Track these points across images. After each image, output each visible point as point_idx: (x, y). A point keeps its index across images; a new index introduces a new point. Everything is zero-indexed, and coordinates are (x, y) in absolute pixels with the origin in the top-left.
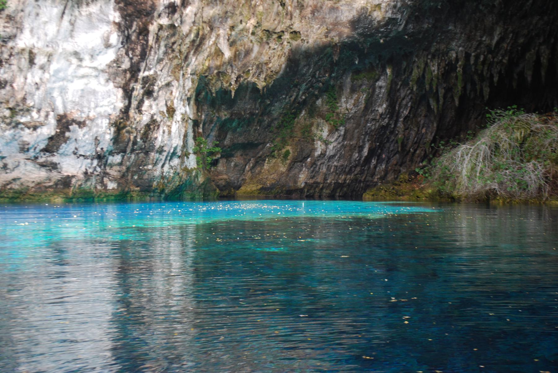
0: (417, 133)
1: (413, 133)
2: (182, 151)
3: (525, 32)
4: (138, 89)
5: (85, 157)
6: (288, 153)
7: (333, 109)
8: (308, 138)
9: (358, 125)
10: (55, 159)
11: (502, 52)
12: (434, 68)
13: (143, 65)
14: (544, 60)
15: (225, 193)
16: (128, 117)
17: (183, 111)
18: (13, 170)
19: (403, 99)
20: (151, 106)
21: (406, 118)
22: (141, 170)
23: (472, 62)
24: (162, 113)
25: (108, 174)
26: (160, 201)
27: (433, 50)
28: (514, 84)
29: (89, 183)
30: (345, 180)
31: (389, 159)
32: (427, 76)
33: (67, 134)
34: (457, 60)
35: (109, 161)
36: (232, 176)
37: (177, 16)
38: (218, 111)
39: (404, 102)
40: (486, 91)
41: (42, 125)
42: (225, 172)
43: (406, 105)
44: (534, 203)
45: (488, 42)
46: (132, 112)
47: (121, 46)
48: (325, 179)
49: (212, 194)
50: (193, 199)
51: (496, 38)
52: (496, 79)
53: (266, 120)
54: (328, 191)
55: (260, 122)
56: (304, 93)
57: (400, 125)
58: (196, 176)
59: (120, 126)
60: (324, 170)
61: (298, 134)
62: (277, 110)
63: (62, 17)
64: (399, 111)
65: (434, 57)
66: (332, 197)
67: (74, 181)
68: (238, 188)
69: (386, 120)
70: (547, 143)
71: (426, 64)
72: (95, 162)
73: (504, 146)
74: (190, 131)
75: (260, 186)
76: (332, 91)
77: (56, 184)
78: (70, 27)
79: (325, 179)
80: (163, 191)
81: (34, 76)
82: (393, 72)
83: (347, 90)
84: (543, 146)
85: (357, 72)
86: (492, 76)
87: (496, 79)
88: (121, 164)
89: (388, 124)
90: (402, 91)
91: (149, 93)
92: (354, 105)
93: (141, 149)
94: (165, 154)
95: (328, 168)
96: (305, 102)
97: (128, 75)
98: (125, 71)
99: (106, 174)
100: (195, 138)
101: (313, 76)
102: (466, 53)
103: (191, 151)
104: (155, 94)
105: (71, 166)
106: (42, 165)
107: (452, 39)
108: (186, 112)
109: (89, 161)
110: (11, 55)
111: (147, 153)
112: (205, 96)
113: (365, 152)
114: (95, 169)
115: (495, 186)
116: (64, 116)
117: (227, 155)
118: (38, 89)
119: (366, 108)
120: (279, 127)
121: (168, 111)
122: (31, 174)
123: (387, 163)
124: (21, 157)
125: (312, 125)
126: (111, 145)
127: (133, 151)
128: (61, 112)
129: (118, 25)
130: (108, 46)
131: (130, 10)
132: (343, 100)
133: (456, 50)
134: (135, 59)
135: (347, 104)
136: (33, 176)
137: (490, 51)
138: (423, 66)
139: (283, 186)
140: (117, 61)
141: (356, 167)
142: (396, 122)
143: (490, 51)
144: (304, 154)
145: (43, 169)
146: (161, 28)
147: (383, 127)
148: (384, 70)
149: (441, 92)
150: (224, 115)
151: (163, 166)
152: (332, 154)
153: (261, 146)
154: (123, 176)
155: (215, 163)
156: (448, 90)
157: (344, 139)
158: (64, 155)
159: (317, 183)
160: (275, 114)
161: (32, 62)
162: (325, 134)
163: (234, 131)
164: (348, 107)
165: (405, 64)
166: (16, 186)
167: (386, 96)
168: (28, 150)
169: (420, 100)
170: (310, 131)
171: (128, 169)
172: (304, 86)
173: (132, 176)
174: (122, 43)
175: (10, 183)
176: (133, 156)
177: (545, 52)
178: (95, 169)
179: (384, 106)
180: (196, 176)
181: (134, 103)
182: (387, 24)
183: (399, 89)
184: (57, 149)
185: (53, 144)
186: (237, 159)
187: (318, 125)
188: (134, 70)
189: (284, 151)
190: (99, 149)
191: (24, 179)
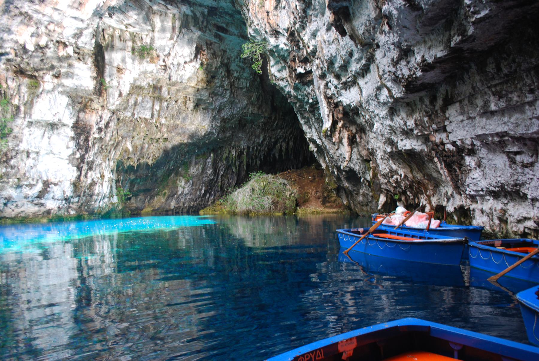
0: (228, 182)
1: (226, 182)
3: (275, 136)
4: (85, 167)
5: (58, 200)
6: (165, 193)
7: (186, 173)
8: (175, 186)
9: (199, 179)
10: (42, 201)
11: (264, 145)
12: (234, 153)
13: (86, 156)
14: (284, 149)
15: (135, 213)
16: (80, 181)
18: (21, 207)
20: (92, 175)
21: (222, 175)
23: (251, 150)
24: (98, 178)
25: (71, 207)
26: (99, 219)
27: (232, 145)
28: (271, 160)
29: (60, 212)
31: (215, 194)
34: (244, 149)
36: (139, 205)
37: (103, 133)
38: (130, 175)
40: (258, 163)
42: (134, 203)
44: (267, 215)
45: (258, 141)
46: (82, 178)
48: (184, 204)
49: (127, 214)
50: (116, 217)
51: (261, 140)
52: (262, 157)
54: (186, 210)
56: (173, 166)
57: (220, 179)
58: (118, 206)
59: (76, 185)
60: (183, 200)
61: (170, 184)
62: (160, 173)
63: (44, 135)
65: (233, 148)
66: (188, 213)
67: (52, 211)
68: (142, 210)
70: (274, 188)
71: (230, 151)
72: (64, 202)
73: (256, 189)
75: (152, 209)
76: (187, 165)
77: (43, 213)
79: (184, 204)
80: (100, 214)
81: (30, 162)
83: (193, 164)
84: (273, 189)
85: (198, 155)
86: (261, 156)
87: (262, 157)
88: (78, 202)
89: (213, 179)
91: (90, 168)
94: (100, 196)
95: (185, 199)
96: (173, 169)
97: (79, 161)
98: (78, 159)
99: (70, 207)
100: (116, 188)
101: (177, 158)
103: (115, 194)
104: (94, 169)
105: (51, 204)
106: (36, 204)
107: (241, 140)
110: (17, 154)
111: (91, 196)
112: (121, 169)
113: (203, 191)
114: (64, 205)
115: (251, 208)
116: (47, 181)
117: (136, 195)
118: (32, 168)
119: (202, 172)
120: (162, 181)
121: (101, 177)
122: (30, 209)
123: (214, 196)
124: (25, 201)
125: (177, 180)
127: (84, 196)
128: (45, 179)
129: (73, 138)
131: (79, 131)
132: (191, 168)
133: (243, 145)
134: (82, 153)
135: (193, 170)
137: (259, 145)
138: (228, 152)
139: (164, 208)
140: (74, 154)
141: (199, 198)
143: (259, 145)
145: (37, 206)
146: (95, 138)
148: (210, 155)
149: (237, 164)
150: (132, 177)
151: (100, 202)
154: (80, 207)
155: (129, 199)
156: (241, 163)
157: (193, 185)
158: (47, 199)
159: (180, 207)
160: (159, 175)
161: (28, 156)
162: (183, 183)
163: (139, 184)
165: (220, 151)
166: (23, 215)
167: (211, 166)
168: (28, 197)
169: (228, 168)
170: (176, 183)
171: (82, 204)
172: (172, 162)
175: (20, 213)
176: (84, 198)
177: (284, 145)
180: (118, 206)
181: (83, 173)
182: (209, 134)
184: (44, 196)
185: (41, 195)
186: (141, 197)
187: (180, 180)
188: (82, 158)
189: (164, 192)
190: (65, 196)
191: (27, 211)
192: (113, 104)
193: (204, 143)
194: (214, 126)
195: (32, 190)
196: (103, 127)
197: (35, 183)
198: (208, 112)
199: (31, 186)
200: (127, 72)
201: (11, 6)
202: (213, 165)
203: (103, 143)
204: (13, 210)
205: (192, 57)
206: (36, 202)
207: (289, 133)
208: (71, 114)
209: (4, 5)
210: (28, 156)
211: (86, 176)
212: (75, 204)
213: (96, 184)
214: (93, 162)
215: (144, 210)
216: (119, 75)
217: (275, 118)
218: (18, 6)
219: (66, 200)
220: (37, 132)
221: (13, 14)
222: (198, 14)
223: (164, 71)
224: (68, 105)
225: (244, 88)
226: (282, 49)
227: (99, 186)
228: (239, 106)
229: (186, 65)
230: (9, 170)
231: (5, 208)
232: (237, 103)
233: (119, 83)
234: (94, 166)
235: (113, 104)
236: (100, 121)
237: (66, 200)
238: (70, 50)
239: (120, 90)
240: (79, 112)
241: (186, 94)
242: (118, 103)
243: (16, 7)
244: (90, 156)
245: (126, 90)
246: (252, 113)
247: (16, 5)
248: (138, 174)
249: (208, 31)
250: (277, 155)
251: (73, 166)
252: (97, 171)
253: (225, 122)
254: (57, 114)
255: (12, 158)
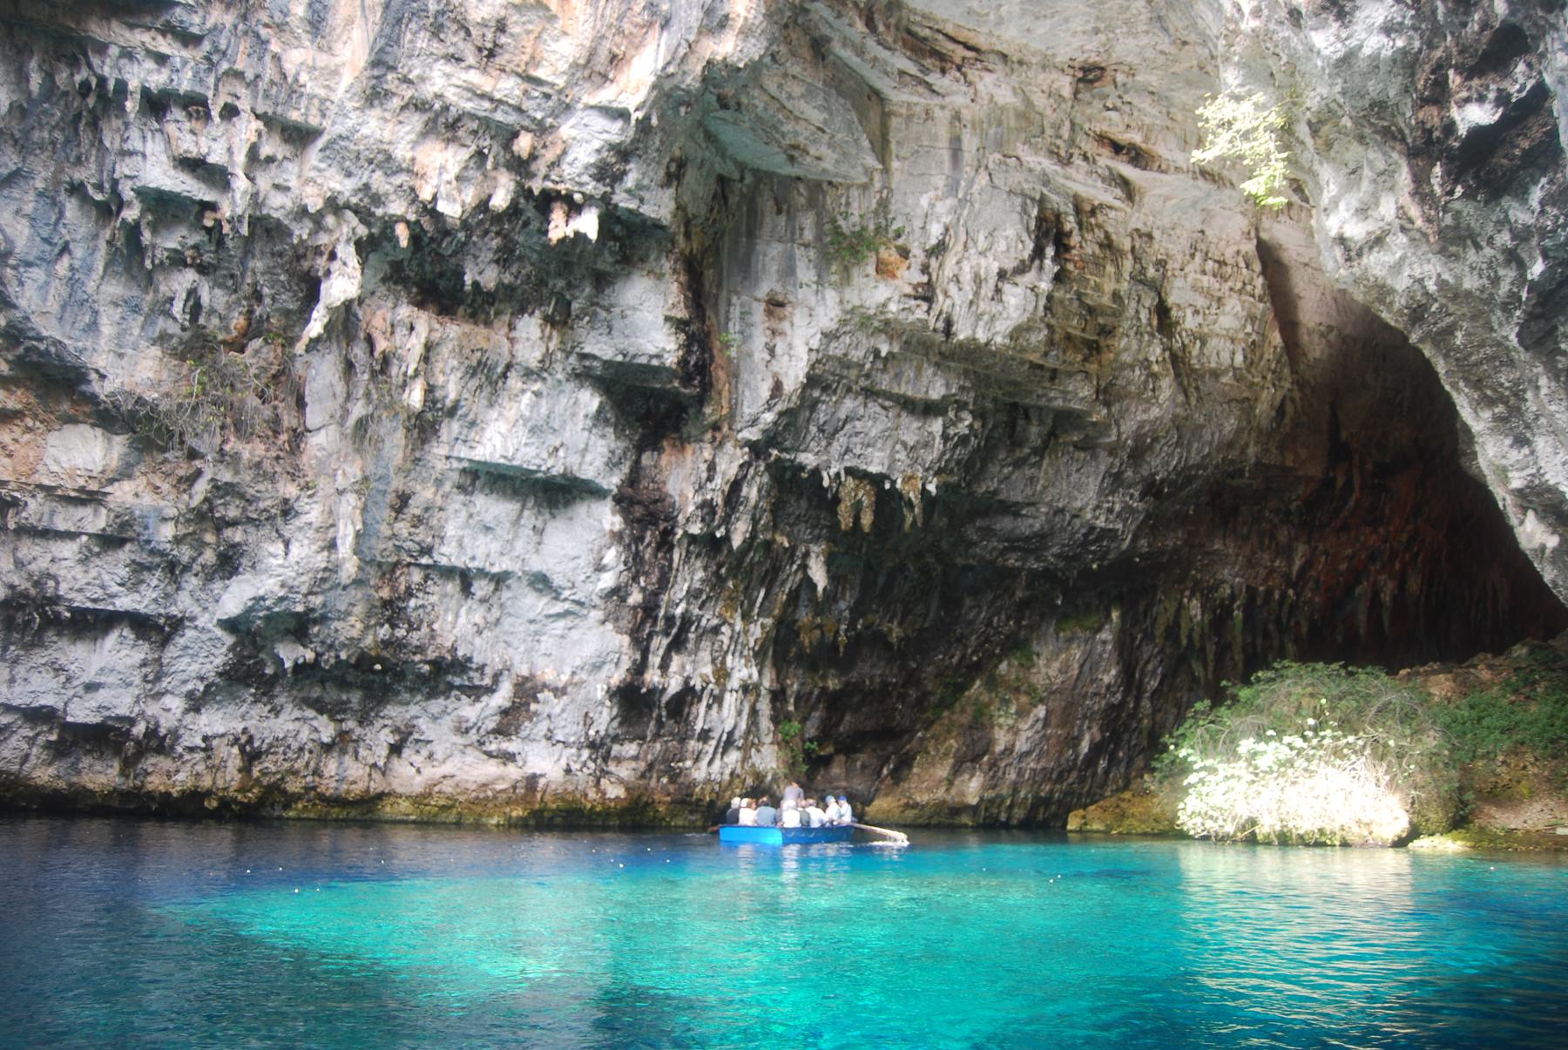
2: (746, 739)
10: (511, 746)
14: (1386, 598)
17: (744, 673)
19: (1148, 662)
22: (673, 769)
23: (1259, 602)
30: (1051, 792)
32: (1183, 624)
33: (533, 707)
34: (1233, 597)
35: (613, 753)
38: (824, 678)
39: (1150, 667)
41: (490, 690)
43: (1154, 672)
46: (652, 677)
47: (622, 567)
51: (1298, 564)
52: (1304, 629)
53: (913, 693)
55: (902, 697)
56: (974, 653)
57: (1146, 704)
60: (1012, 776)
64: (1141, 680)
67: (542, 782)
69: (1119, 696)
71: (1181, 605)
72: (586, 753)
74: (764, 707)
78: (536, 538)
82: (1123, 617)
86: (1298, 623)
88: (636, 758)
89: (1123, 703)
90: (1145, 648)
91: (677, 645)
92: (1060, 671)
93: (671, 734)
94: (713, 743)
95: (1020, 773)
98: (634, 608)
99: (605, 773)
100: (775, 719)
101: (989, 624)
102: (1248, 587)
104: (690, 646)
106: (490, 755)
108: (750, 677)
109: (574, 750)
110: (426, 578)
111: (682, 741)
113: (1085, 747)
118: (479, 632)
126: (615, 724)
128: (525, 672)
129: (617, 537)
130: (600, 568)
133: (1231, 578)
136: (476, 772)
140: (618, 593)
141: (1070, 771)
142: (1138, 700)
144: (978, 750)
145: (493, 761)
146: (693, 539)
147: (1112, 707)
148: (1108, 616)
149: (1211, 649)
151: (710, 763)
152: (1025, 748)
153: (906, 737)
154: (643, 776)
161: (466, 589)
164: (1051, 673)
166: (447, 787)
168: (467, 731)
171: (651, 766)
173: (659, 778)
174: (625, 563)
178: (585, 764)
179: (1113, 672)
181: (655, 660)
182: (1098, 540)
183: (1139, 646)
188: (649, 609)
190: (592, 732)
191: (460, 776)
192: (754, 422)
193: (1086, 573)
194: (1117, 507)
195: (479, 706)
196: (719, 500)
197: (487, 681)
198: (1094, 457)
199: (476, 693)
200: (799, 317)
201: (390, 77)
202: (1121, 655)
203: (721, 558)
204: (418, 771)
205: (1026, 255)
206: (493, 747)
207: (1404, 537)
208: (613, 452)
209: (368, 73)
210: (466, 589)
211: (664, 667)
212: (625, 764)
213: (700, 700)
214: (687, 621)
215: (876, 803)
216: (775, 324)
217: (1349, 482)
218: (411, 76)
219: (592, 746)
220: (494, 508)
221: (396, 102)
222: (1040, 101)
223: (925, 306)
224: (599, 418)
225: (1225, 372)
226: (1375, 58)
227: (709, 707)
228: (1207, 437)
229: (1007, 288)
230: (400, 633)
231: (395, 760)
232: (1202, 427)
233: (772, 351)
234: (692, 636)
235: (754, 422)
236: (710, 479)
237: (592, 746)
238: (588, 224)
239: (775, 375)
240: (640, 449)
241: (1010, 394)
242: (769, 417)
243: (406, 80)
244: (677, 599)
245: (794, 373)
246: (1258, 464)
247: (405, 70)
248: (854, 676)
249: (1078, 161)
250: (1362, 618)
251: (619, 631)
252: (705, 656)
253: (1158, 495)
254: (561, 453)
255: (409, 593)
